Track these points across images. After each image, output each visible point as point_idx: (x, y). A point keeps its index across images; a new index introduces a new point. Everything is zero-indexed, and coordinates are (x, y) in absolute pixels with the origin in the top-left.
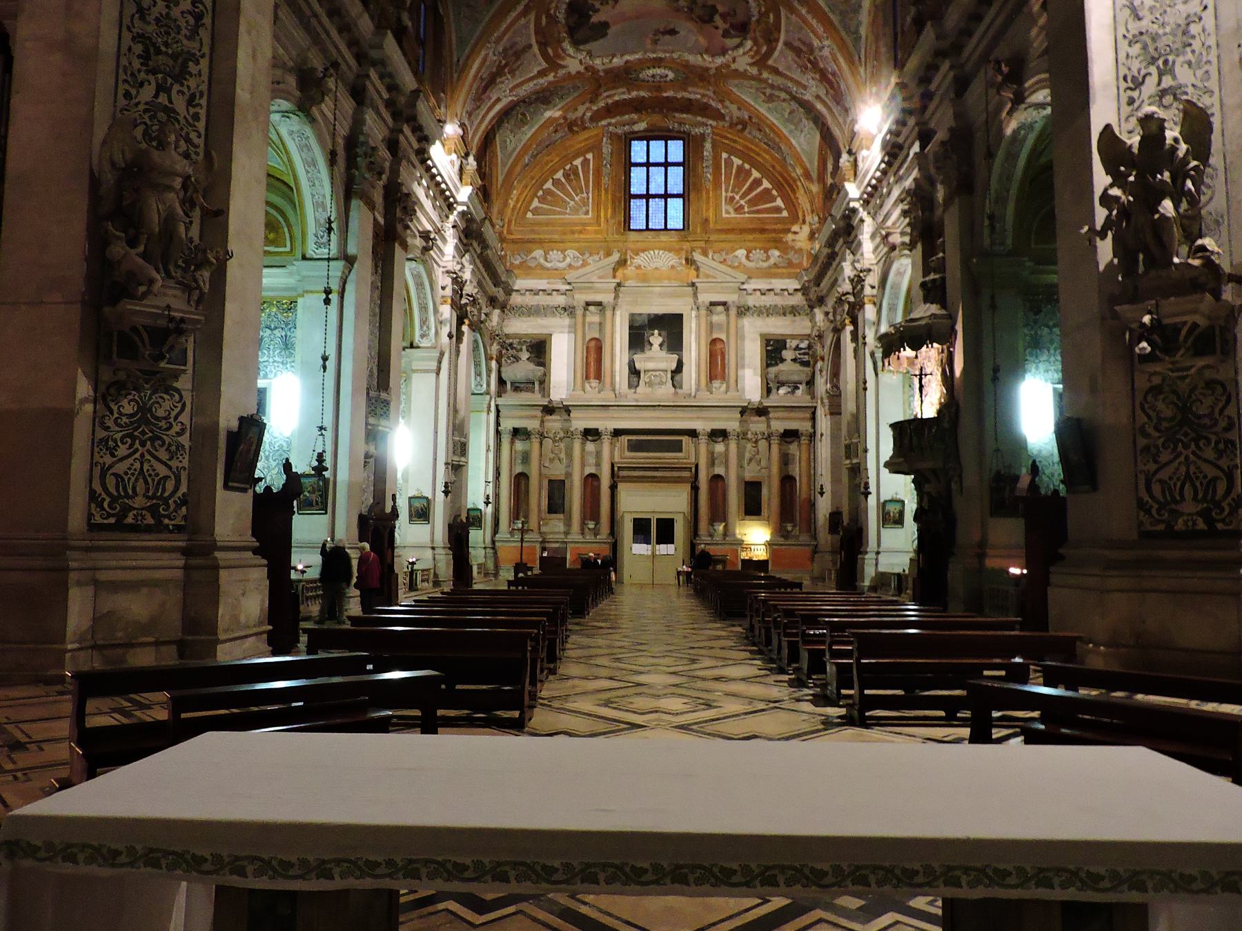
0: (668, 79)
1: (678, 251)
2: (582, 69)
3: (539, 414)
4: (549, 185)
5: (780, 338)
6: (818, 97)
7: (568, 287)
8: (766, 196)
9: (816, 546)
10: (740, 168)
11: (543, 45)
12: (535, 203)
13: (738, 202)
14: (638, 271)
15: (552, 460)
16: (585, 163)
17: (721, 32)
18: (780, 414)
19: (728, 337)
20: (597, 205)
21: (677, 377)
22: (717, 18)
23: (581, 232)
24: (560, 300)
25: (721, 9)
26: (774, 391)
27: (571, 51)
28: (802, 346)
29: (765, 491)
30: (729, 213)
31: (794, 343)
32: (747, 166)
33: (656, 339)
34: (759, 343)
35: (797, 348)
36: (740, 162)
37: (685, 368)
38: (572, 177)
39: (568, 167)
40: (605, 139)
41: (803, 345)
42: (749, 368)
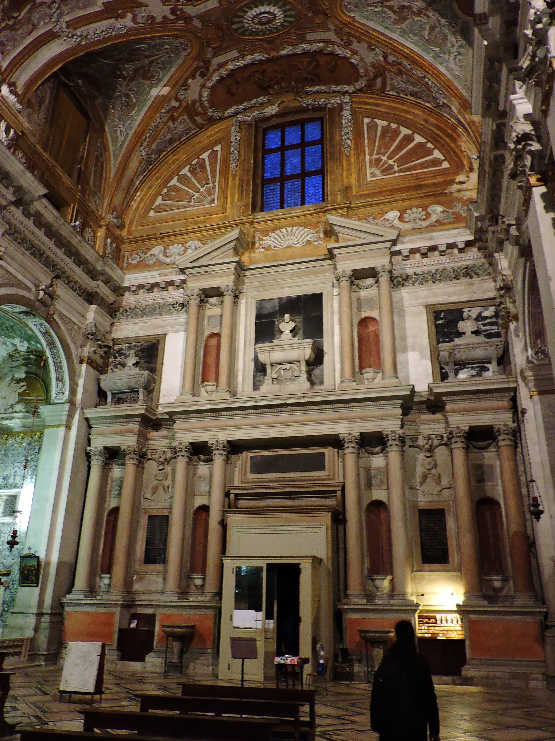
1: (314, 225)
3: (136, 427)
4: (174, 182)
7: (183, 277)
9: (546, 615)
12: (159, 201)
13: (385, 163)
14: (267, 252)
15: (155, 490)
21: (317, 371)
24: (175, 295)
26: (451, 375)
28: (486, 314)
29: (451, 524)
31: (475, 312)
32: (394, 126)
34: (424, 317)
35: (479, 318)
36: (385, 123)
37: (327, 359)
39: (194, 162)
40: (233, 128)
42: (414, 349)
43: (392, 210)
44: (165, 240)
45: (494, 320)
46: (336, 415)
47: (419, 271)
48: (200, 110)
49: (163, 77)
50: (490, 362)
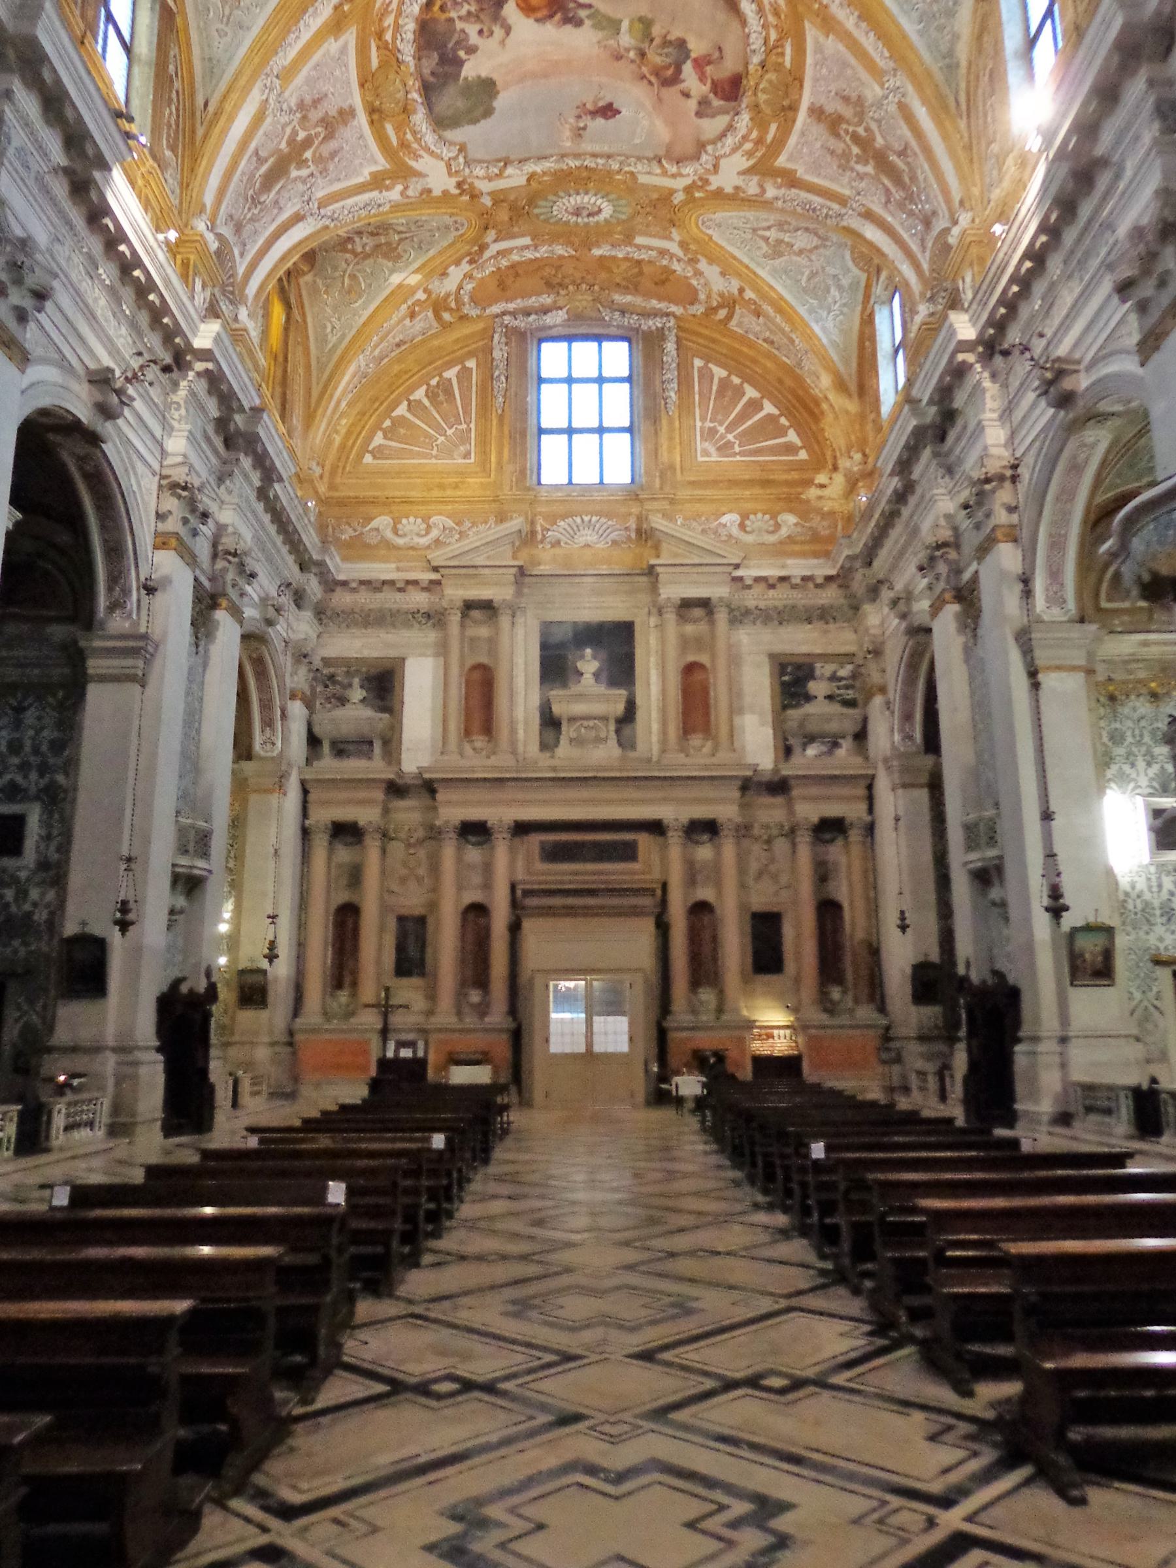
0: (601, 218)
2: (450, 184)
3: (379, 795)
5: (801, 660)
6: (868, 215)
7: (434, 576)
8: (770, 427)
9: (888, 1028)
10: (724, 384)
11: (375, 113)
12: (379, 440)
13: (722, 437)
15: (403, 880)
16: (465, 373)
17: (692, 104)
18: (814, 791)
19: (713, 657)
20: (483, 442)
21: (627, 731)
22: (688, 68)
23: (456, 487)
24: (419, 599)
25: (697, 47)
26: (797, 750)
27: (430, 138)
28: (842, 673)
30: (706, 453)
31: (828, 669)
32: (736, 380)
33: (589, 663)
35: (834, 678)
37: (640, 715)
38: (442, 398)
39: (434, 382)
40: (496, 336)
41: (844, 672)
42: (753, 712)
43: (730, 511)
44: (394, 508)
45: (850, 682)
46: (660, 794)
47: (762, 605)
48: (453, 305)
49: (414, 260)
50: (843, 737)
